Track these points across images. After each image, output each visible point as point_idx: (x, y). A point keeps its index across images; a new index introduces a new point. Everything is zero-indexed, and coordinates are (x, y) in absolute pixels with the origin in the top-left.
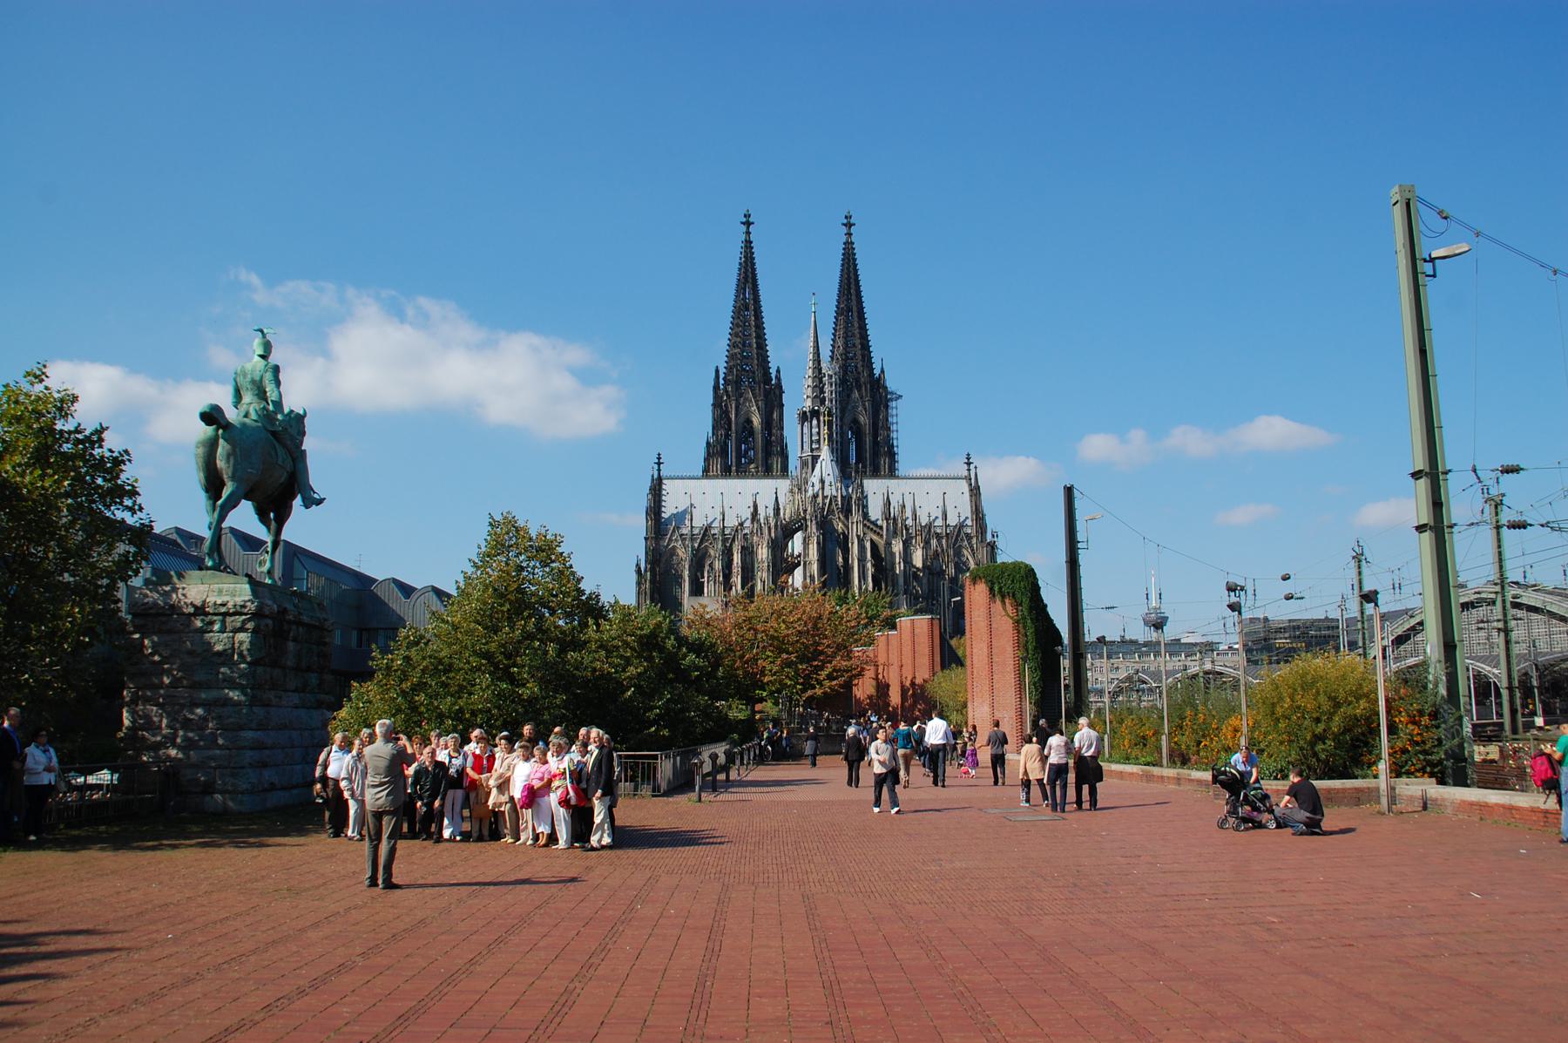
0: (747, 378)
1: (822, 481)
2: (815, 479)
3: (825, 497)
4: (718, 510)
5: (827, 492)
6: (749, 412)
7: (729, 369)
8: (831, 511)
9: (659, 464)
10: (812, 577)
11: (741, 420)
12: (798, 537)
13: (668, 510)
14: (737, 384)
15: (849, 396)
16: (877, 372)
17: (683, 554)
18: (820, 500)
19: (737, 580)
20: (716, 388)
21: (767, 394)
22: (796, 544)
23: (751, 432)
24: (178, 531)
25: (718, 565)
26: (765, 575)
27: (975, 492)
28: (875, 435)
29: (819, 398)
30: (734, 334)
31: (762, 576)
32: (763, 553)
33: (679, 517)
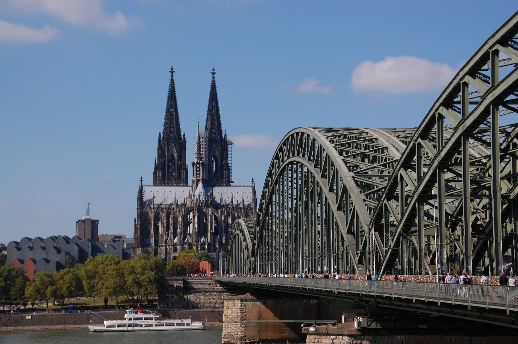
0: (172, 138)
2: (197, 195)
3: (200, 201)
5: (201, 199)
6: (172, 152)
8: (202, 205)
9: (141, 181)
10: (195, 228)
11: (170, 155)
12: (191, 214)
13: (145, 199)
14: (168, 140)
15: (212, 146)
16: (223, 135)
17: (152, 216)
18: (199, 201)
19: (171, 227)
20: (159, 141)
22: (191, 216)
24: (66, 236)
25: (164, 221)
26: (181, 226)
27: (254, 192)
28: (222, 162)
29: (200, 158)
31: (180, 227)
32: (180, 220)
33: (150, 201)
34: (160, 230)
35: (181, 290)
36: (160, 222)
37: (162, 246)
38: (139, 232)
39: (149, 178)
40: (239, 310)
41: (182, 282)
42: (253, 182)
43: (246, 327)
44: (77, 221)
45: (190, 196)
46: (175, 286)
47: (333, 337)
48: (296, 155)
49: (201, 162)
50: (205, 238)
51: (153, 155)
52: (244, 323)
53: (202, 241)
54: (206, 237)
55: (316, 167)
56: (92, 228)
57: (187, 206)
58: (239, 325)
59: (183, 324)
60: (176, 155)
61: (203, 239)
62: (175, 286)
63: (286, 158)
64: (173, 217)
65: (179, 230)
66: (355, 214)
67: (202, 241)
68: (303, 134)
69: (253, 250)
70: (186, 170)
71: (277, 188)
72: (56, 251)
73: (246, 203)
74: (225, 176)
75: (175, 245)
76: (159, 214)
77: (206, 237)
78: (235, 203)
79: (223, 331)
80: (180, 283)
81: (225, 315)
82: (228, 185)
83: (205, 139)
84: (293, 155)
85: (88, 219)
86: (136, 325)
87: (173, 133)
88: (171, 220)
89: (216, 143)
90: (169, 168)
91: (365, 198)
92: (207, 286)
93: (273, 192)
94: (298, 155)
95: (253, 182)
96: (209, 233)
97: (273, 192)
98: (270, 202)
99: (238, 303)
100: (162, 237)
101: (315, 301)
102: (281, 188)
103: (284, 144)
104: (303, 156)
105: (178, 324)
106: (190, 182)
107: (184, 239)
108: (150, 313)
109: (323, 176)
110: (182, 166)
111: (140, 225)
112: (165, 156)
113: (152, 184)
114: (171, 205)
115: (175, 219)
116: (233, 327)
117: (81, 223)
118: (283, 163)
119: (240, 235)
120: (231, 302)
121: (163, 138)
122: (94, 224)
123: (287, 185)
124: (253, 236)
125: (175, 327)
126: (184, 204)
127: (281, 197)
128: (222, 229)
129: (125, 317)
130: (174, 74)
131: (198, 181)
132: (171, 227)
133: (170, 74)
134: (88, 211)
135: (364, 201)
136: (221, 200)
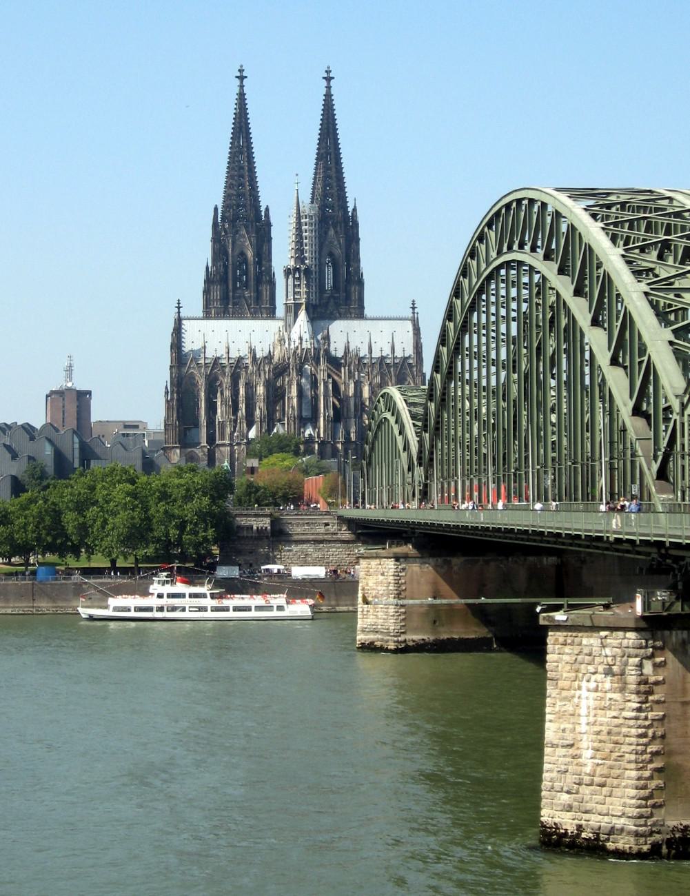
0: (241, 216)
1: (301, 339)
4: (224, 345)
6: (243, 244)
7: (226, 206)
9: (179, 308)
11: (237, 252)
15: (326, 233)
16: (350, 209)
17: (202, 382)
18: (299, 351)
19: (242, 406)
20: (215, 224)
21: (258, 231)
23: (245, 261)
24: (28, 424)
25: (228, 393)
26: (262, 404)
28: (348, 266)
29: (300, 258)
30: (230, 176)
32: (261, 390)
34: (219, 411)
35: (267, 537)
36: (219, 394)
37: (223, 445)
38: (175, 415)
39: (194, 303)
40: (391, 579)
41: (268, 521)
42: (413, 308)
43: (406, 615)
44: (48, 392)
45: (281, 341)
46: (255, 528)
47: (603, 634)
48: (515, 247)
49: (303, 267)
50: (314, 428)
51: (201, 254)
52: (402, 606)
53: (306, 435)
54: (315, 426)
55: (561, 271)
56: (78, 407)
57: (276, 359)
58: (392, 610)
59: (270, 608)
60: (250, 254)
61: (309, 431)
62: (255, 528)
63: (494, 254)
64: (246, 384)
65: (258, 412)
66: (650, 373)
67: (306, 435)
68: (532, 201)
69: (420, 452)
70: (272, 283)
71: (475, 320)
72: (9, 456)
73: (399, 354)
74: (354, 296)
75: (249, 442)
76: (216, 379)
77: (315, 426)
78: (376, 354)
79: (360, 621)
80: (265, 523)
81: (363, 589)
82: (360, 315)
83: (311, 217)
84: (510, 248)
85: (69, 389)
86: (174, 609)
87: (244, 206)
88: (242, 391)
89: (335, 228)
90: (236, 282)
91: (672, 338)
92: (322, 529)
93: (465, 327)
94: (521, 246)
95: (413, 308)
96: (322, 419)
97: (465, 327)
98: (457, 349)
99: (390, 564)
100: (222, 425)
101: (552, 560)
102: (484, 320)
103: (489, 225)
104: (533, 249)
105: (259, 608)
106: (280, 311)
107: (269, 430)
108: (202, 584)
109: (578, 292)
110: (264, 278)
111: (177, 400)
112: (226, 253)
113: (201, 315)
114: (240, 359)
115: (250, 387)
116: (379, 614)
117: (56, 397)
118: (488, 264)
119: (392, 420)
120: (374, 563)
121: (223, 218)
122: (83, 398)
123: (497, 314)
124: (419, 424)
125: (253, 614)
126: (269, 358)
127: (484, 340)
128: (348, 410)
129: (151, 591)
130: (245, 80)
131: (297, 307)
132: (242, 406)
133: (238, 82)
134: (69, 370)
135: (671, 343)
136: (347, 349)
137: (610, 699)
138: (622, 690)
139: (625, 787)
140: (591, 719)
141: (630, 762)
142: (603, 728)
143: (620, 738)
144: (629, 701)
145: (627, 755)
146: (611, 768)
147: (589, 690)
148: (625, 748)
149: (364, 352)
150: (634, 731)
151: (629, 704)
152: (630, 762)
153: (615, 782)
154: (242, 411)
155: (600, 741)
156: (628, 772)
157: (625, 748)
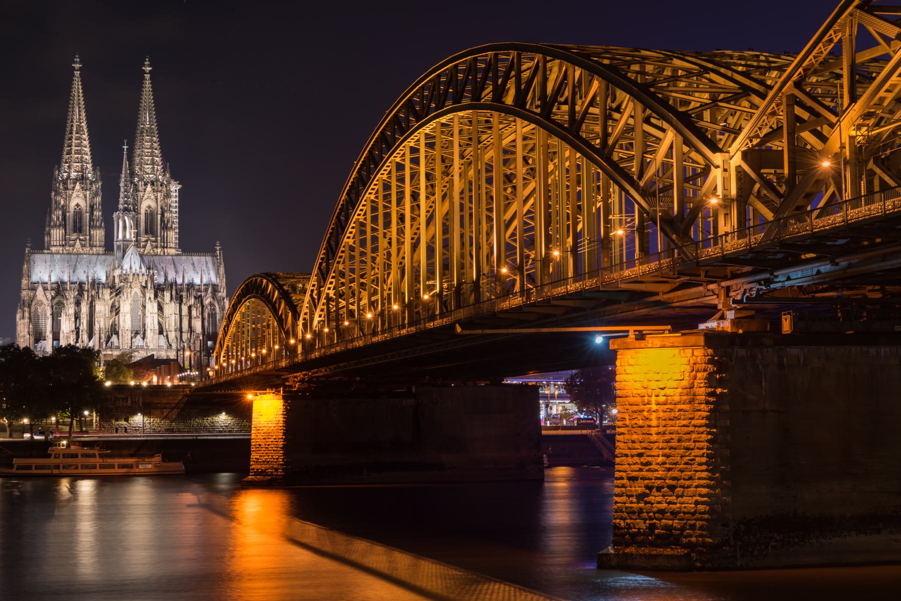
15: (145, 190)
25: (71, 310)
137: (680, 410)
138: (691, 402)
139: (697, 487)
140: (661, 429)
141: (700, 464)
142: (673, 436)
143: (691, 444)
144: (700, 410)
145: (697, 459)
146: (682, 471)
147: (658, 404)
148: (696, 452)
149: (179, 281)
150: (704, 437)
151: (699, 413)
152: (700, 464)
153: (688, 483)
154: (84, 326)
155: (671, 448)
156: (698, 475)
157: (696, 452)
